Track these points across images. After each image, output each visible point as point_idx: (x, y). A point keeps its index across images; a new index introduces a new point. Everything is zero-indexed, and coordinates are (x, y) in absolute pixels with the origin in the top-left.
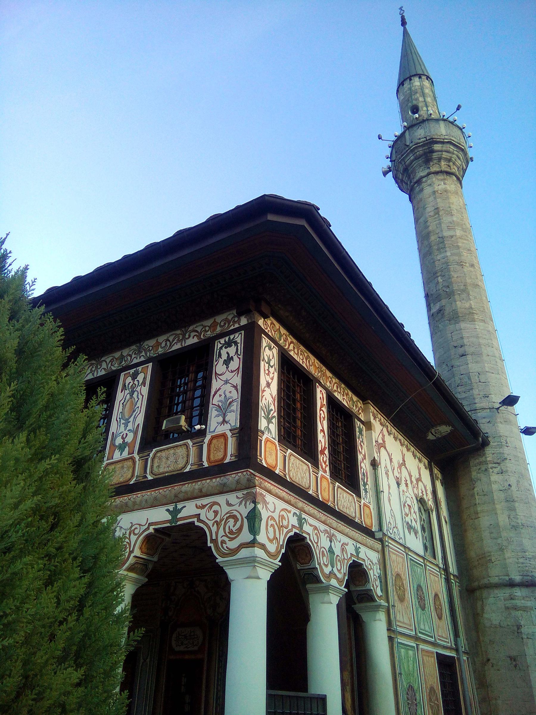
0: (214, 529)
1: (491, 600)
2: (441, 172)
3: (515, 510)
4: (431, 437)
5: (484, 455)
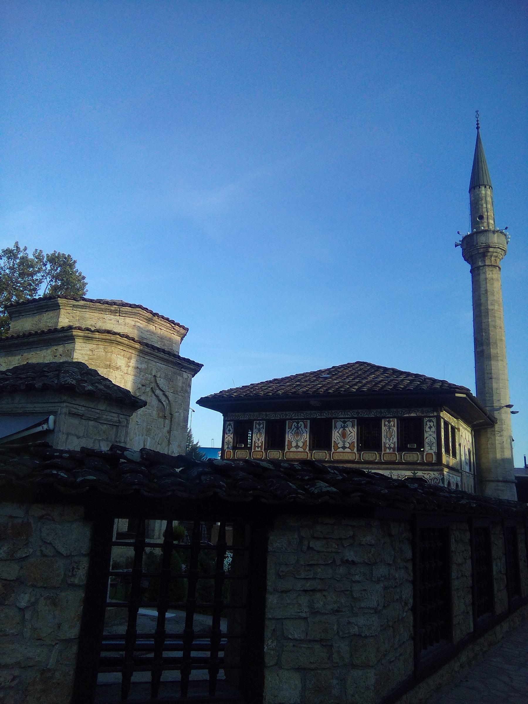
0: (430, 481)
2: (491, 265)
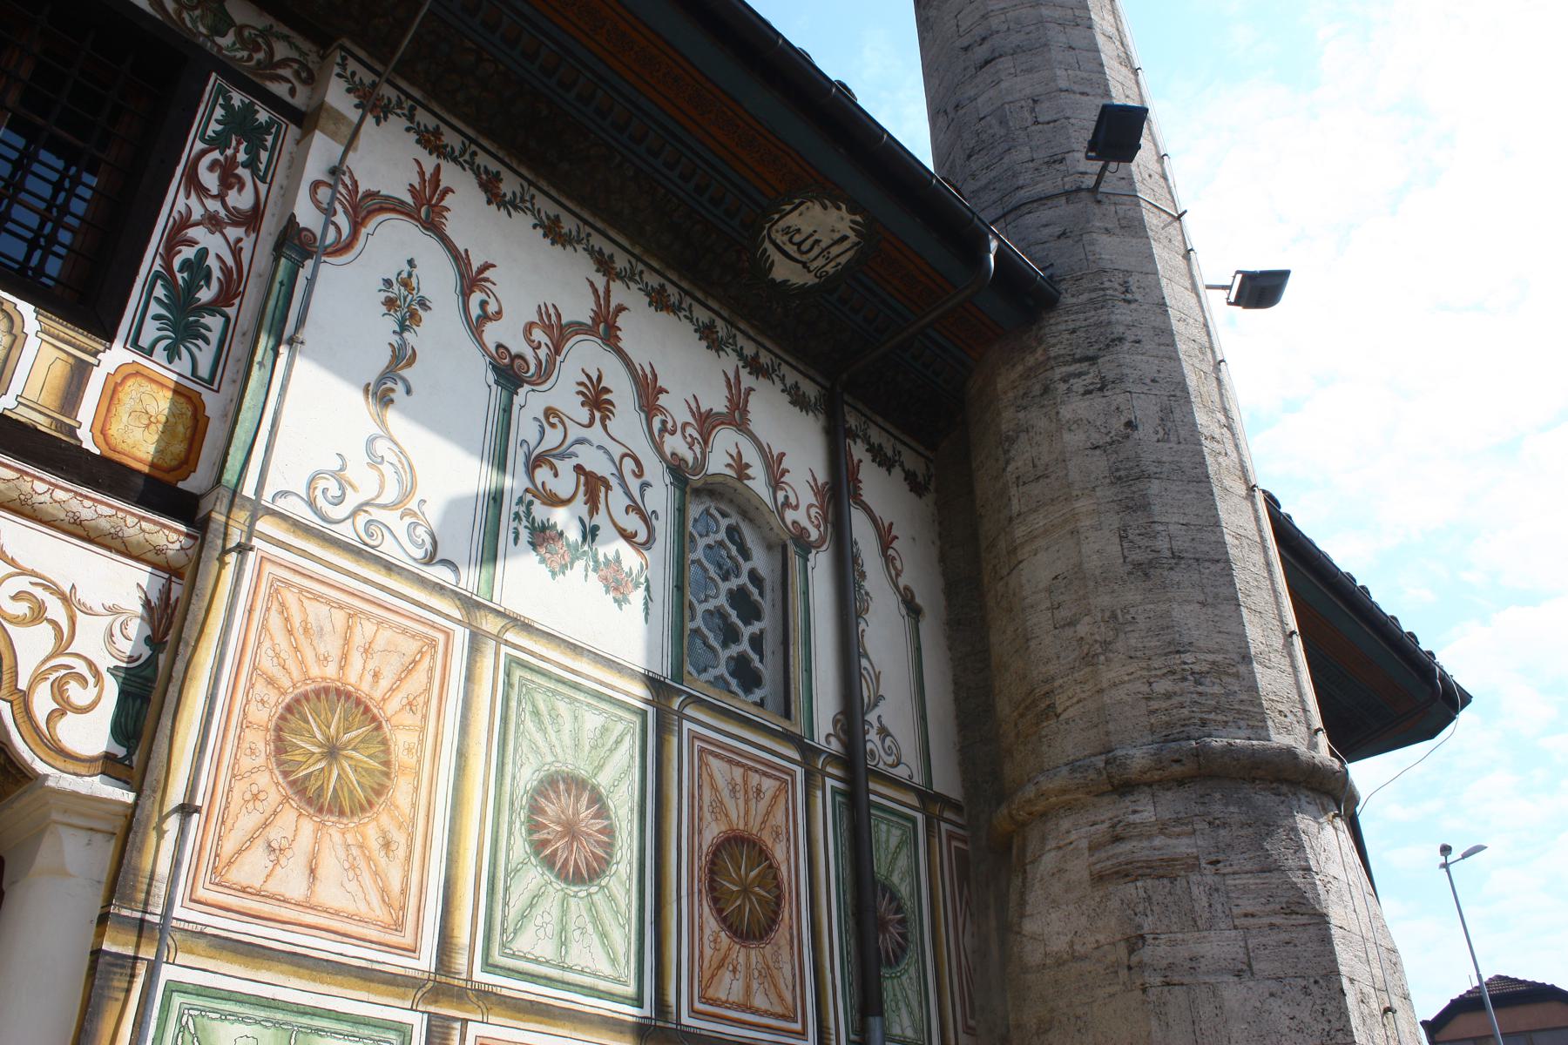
1: (1049, 861)
3: (1145, 507)
4: (783, 271)
5: (1040, 341)
